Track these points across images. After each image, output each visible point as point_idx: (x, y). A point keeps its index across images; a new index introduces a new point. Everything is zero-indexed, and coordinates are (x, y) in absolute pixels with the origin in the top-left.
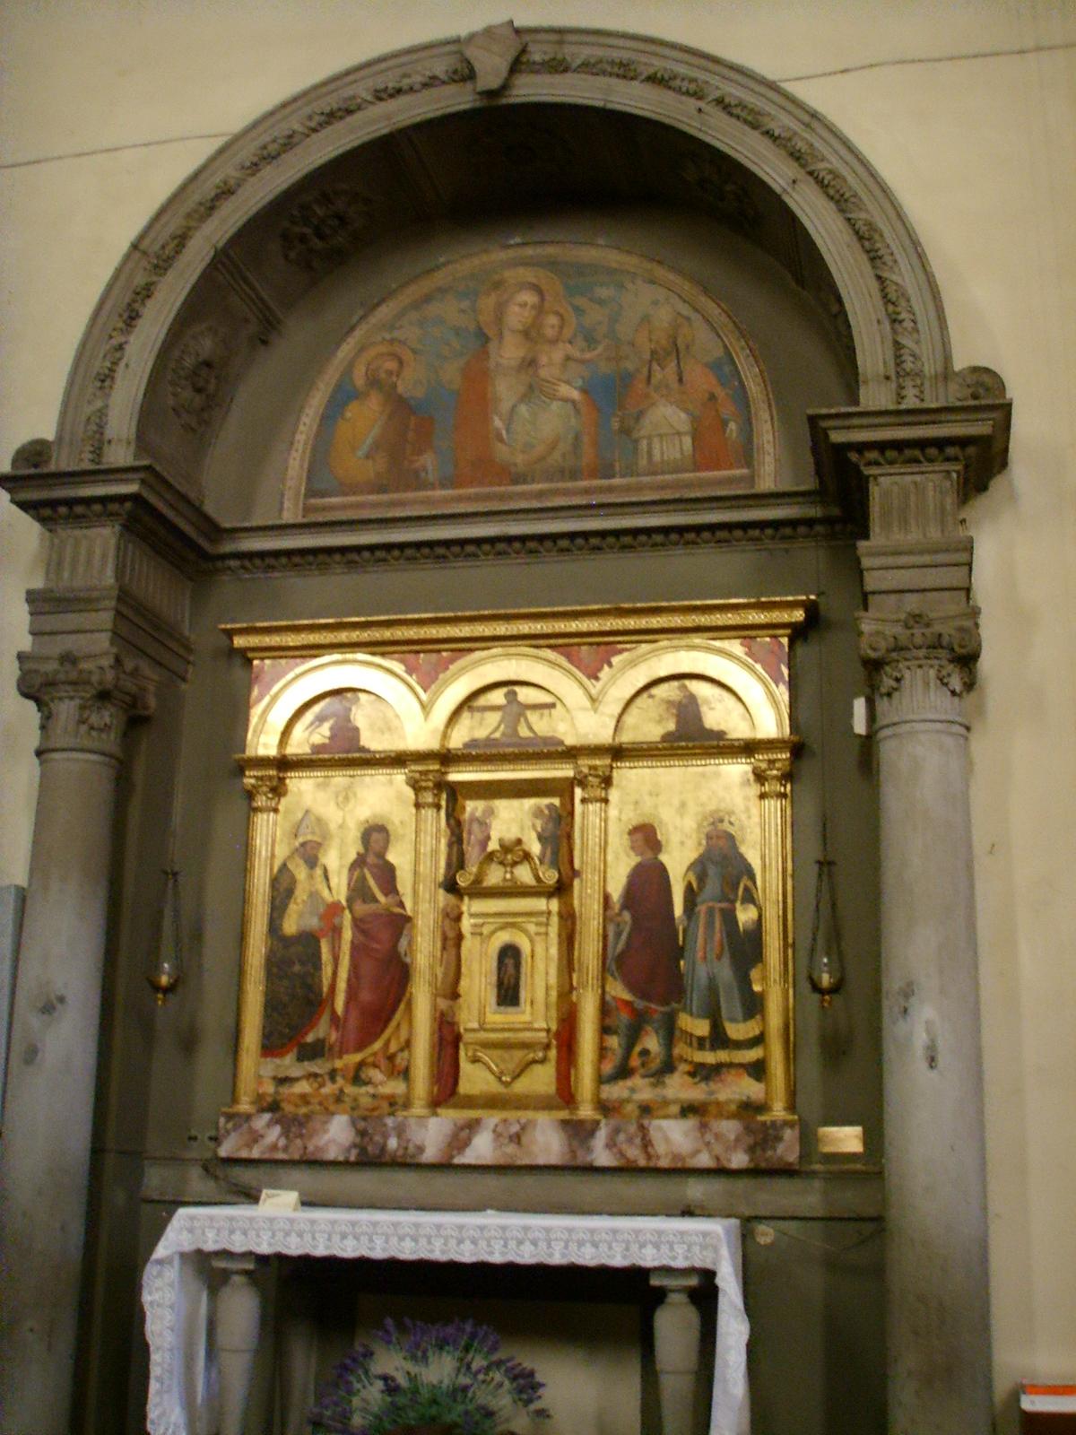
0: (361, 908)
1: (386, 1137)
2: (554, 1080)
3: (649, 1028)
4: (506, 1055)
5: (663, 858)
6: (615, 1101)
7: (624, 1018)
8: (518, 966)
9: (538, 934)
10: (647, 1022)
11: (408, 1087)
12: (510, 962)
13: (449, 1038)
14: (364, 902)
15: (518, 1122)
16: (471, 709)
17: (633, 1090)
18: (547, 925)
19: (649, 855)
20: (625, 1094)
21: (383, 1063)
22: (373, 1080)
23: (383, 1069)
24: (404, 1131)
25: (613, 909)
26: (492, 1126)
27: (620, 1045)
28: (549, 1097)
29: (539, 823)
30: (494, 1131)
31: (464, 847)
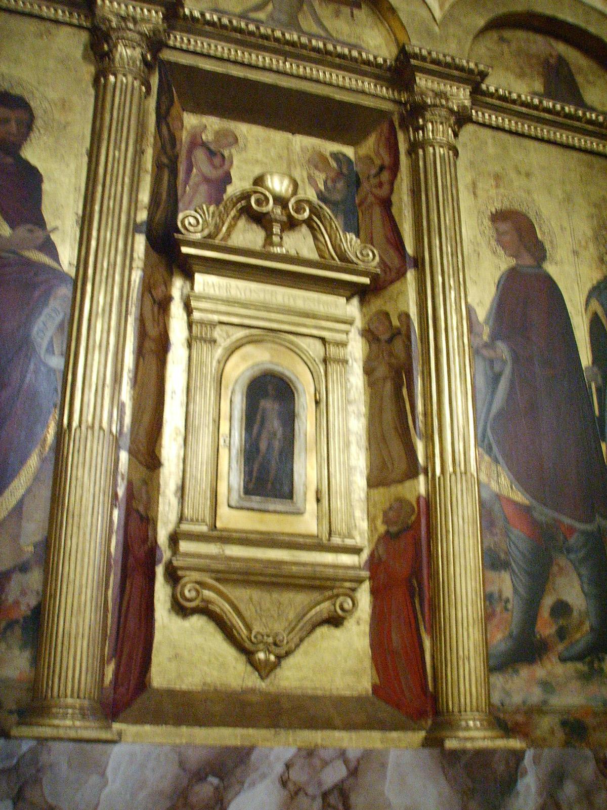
2: (367, 663)
5: (551, 269)
6: (517, 711)
8: (289, 418)
11: (36, 661)
13: (140, 551)
17: (547, 686)
19: (528, 260)
20: (536, 695)
24: (37, 781)
26: (279, 768)
27: (515, 590)
28: (360, 700)
29: (320, 178)
30: (284, 783)
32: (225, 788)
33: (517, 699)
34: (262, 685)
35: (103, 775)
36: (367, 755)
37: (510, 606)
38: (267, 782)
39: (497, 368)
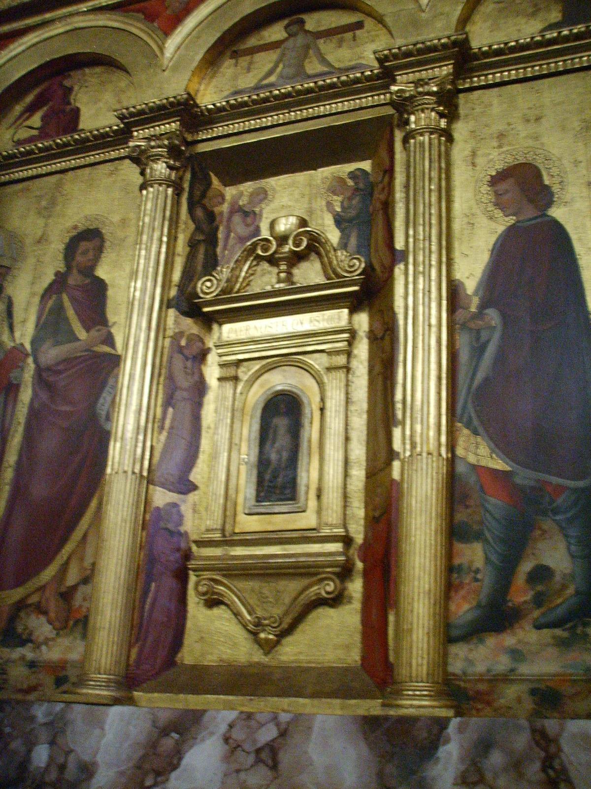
0: (52, 354)
1: (30, 745)
2: (358, 638)
3: (547, 524)
4: (267, 588)
7: (496, 503)
9: (329, 369)
10: (544, 513)
12: (281, 423)
14: (57, 343)
15: (275, 718)
16: (236, 55)
17: (516, 654)
18: (349, 354)
19: (530, 212)
20: (503, 663)
21: (53, 605)
22: (33, 638)
23: (52, 615)
24: (63, 731)
25: (467, 308)
26: (223, 728)
27: (487, 559)
30: (226, 739)
31: (219, 250)
32: (184, 741)
33: (480, 668)
34: (265, 659)
35: (103, 729)
36: (297, 718)
37: (479, 576)
38: (214, 738)
39: (484, 336)
